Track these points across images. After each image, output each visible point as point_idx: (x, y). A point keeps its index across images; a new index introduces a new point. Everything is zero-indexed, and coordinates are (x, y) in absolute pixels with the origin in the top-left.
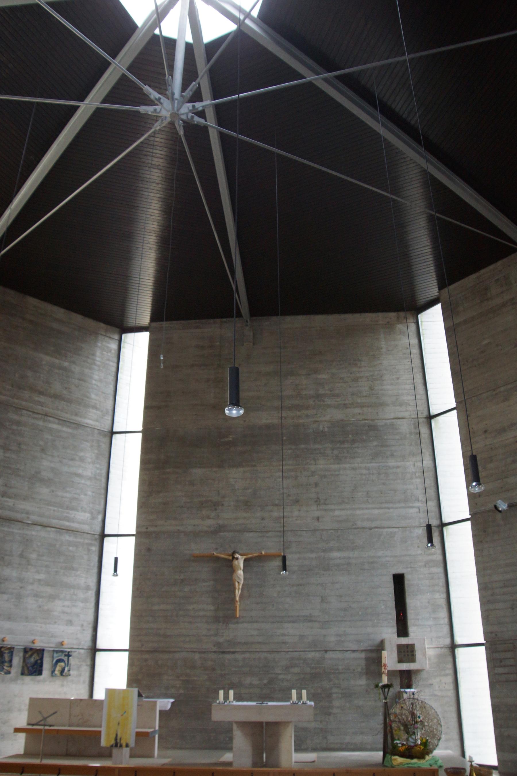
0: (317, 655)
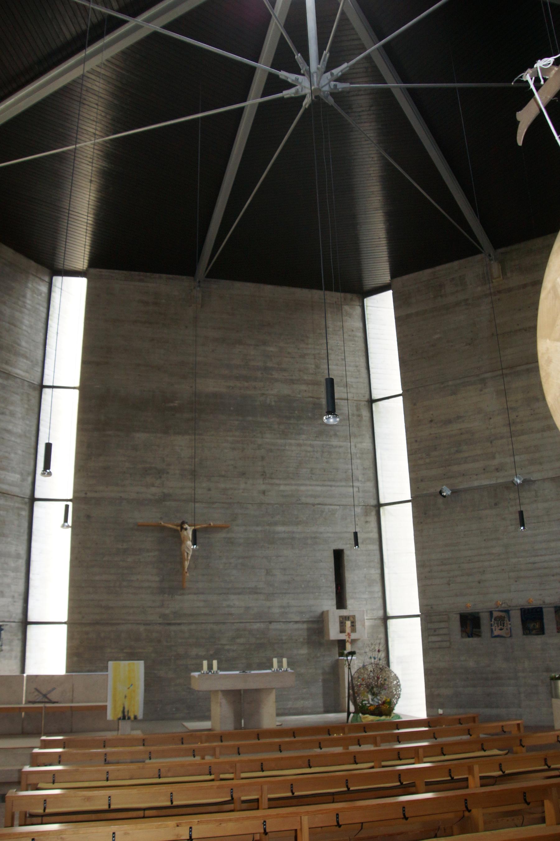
0: (262, 626)
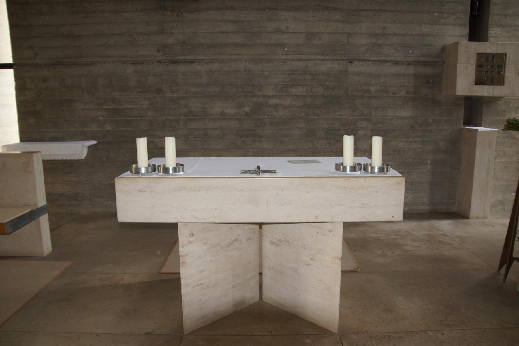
0: (336, 66)
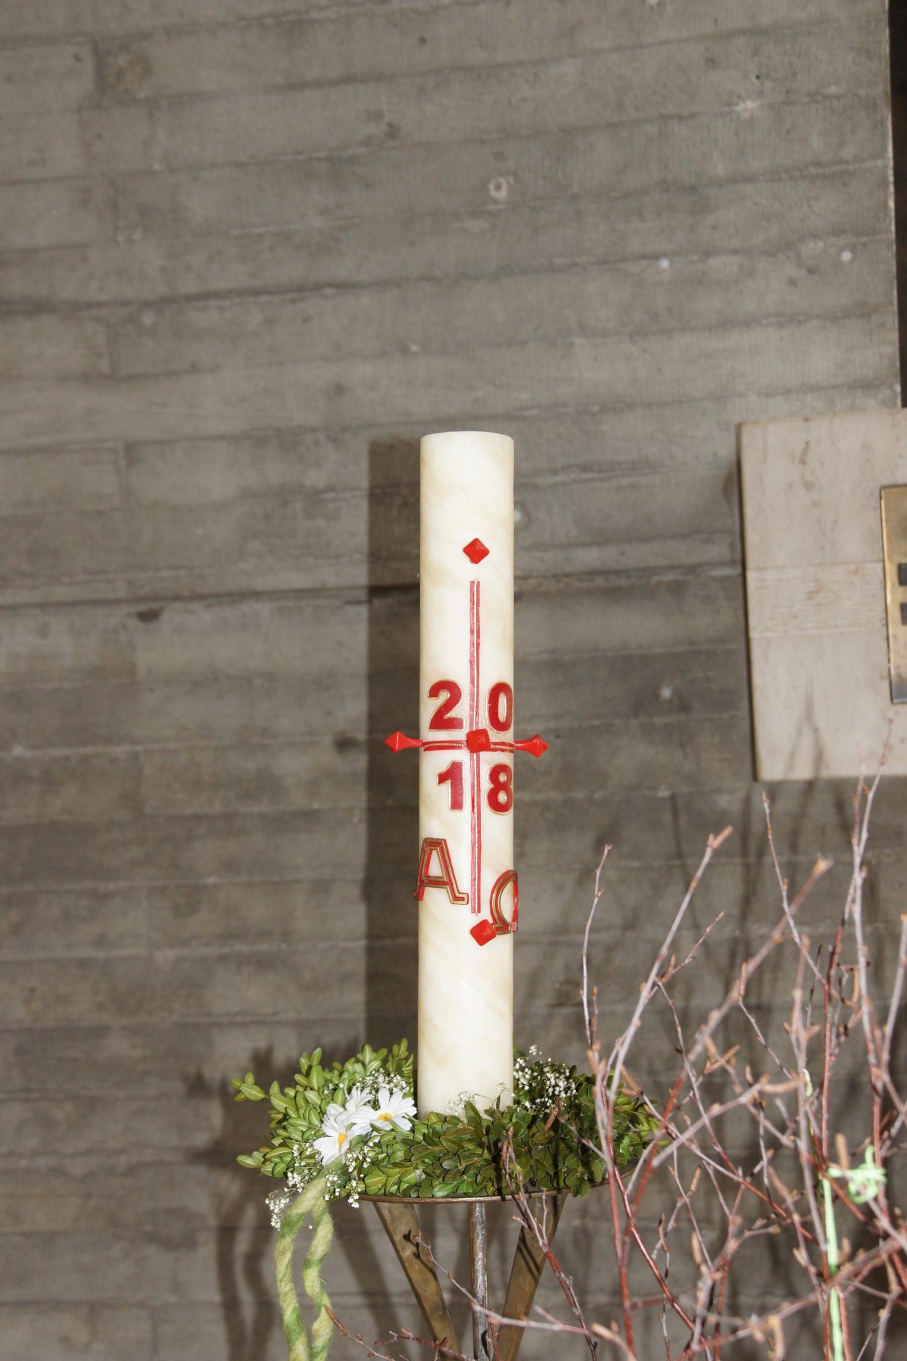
0: (65, 646)
